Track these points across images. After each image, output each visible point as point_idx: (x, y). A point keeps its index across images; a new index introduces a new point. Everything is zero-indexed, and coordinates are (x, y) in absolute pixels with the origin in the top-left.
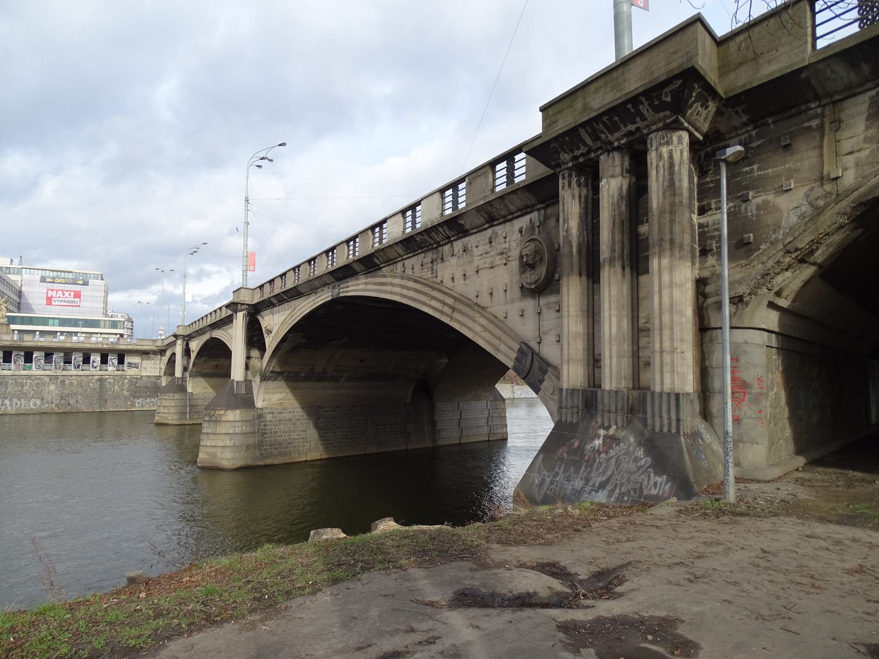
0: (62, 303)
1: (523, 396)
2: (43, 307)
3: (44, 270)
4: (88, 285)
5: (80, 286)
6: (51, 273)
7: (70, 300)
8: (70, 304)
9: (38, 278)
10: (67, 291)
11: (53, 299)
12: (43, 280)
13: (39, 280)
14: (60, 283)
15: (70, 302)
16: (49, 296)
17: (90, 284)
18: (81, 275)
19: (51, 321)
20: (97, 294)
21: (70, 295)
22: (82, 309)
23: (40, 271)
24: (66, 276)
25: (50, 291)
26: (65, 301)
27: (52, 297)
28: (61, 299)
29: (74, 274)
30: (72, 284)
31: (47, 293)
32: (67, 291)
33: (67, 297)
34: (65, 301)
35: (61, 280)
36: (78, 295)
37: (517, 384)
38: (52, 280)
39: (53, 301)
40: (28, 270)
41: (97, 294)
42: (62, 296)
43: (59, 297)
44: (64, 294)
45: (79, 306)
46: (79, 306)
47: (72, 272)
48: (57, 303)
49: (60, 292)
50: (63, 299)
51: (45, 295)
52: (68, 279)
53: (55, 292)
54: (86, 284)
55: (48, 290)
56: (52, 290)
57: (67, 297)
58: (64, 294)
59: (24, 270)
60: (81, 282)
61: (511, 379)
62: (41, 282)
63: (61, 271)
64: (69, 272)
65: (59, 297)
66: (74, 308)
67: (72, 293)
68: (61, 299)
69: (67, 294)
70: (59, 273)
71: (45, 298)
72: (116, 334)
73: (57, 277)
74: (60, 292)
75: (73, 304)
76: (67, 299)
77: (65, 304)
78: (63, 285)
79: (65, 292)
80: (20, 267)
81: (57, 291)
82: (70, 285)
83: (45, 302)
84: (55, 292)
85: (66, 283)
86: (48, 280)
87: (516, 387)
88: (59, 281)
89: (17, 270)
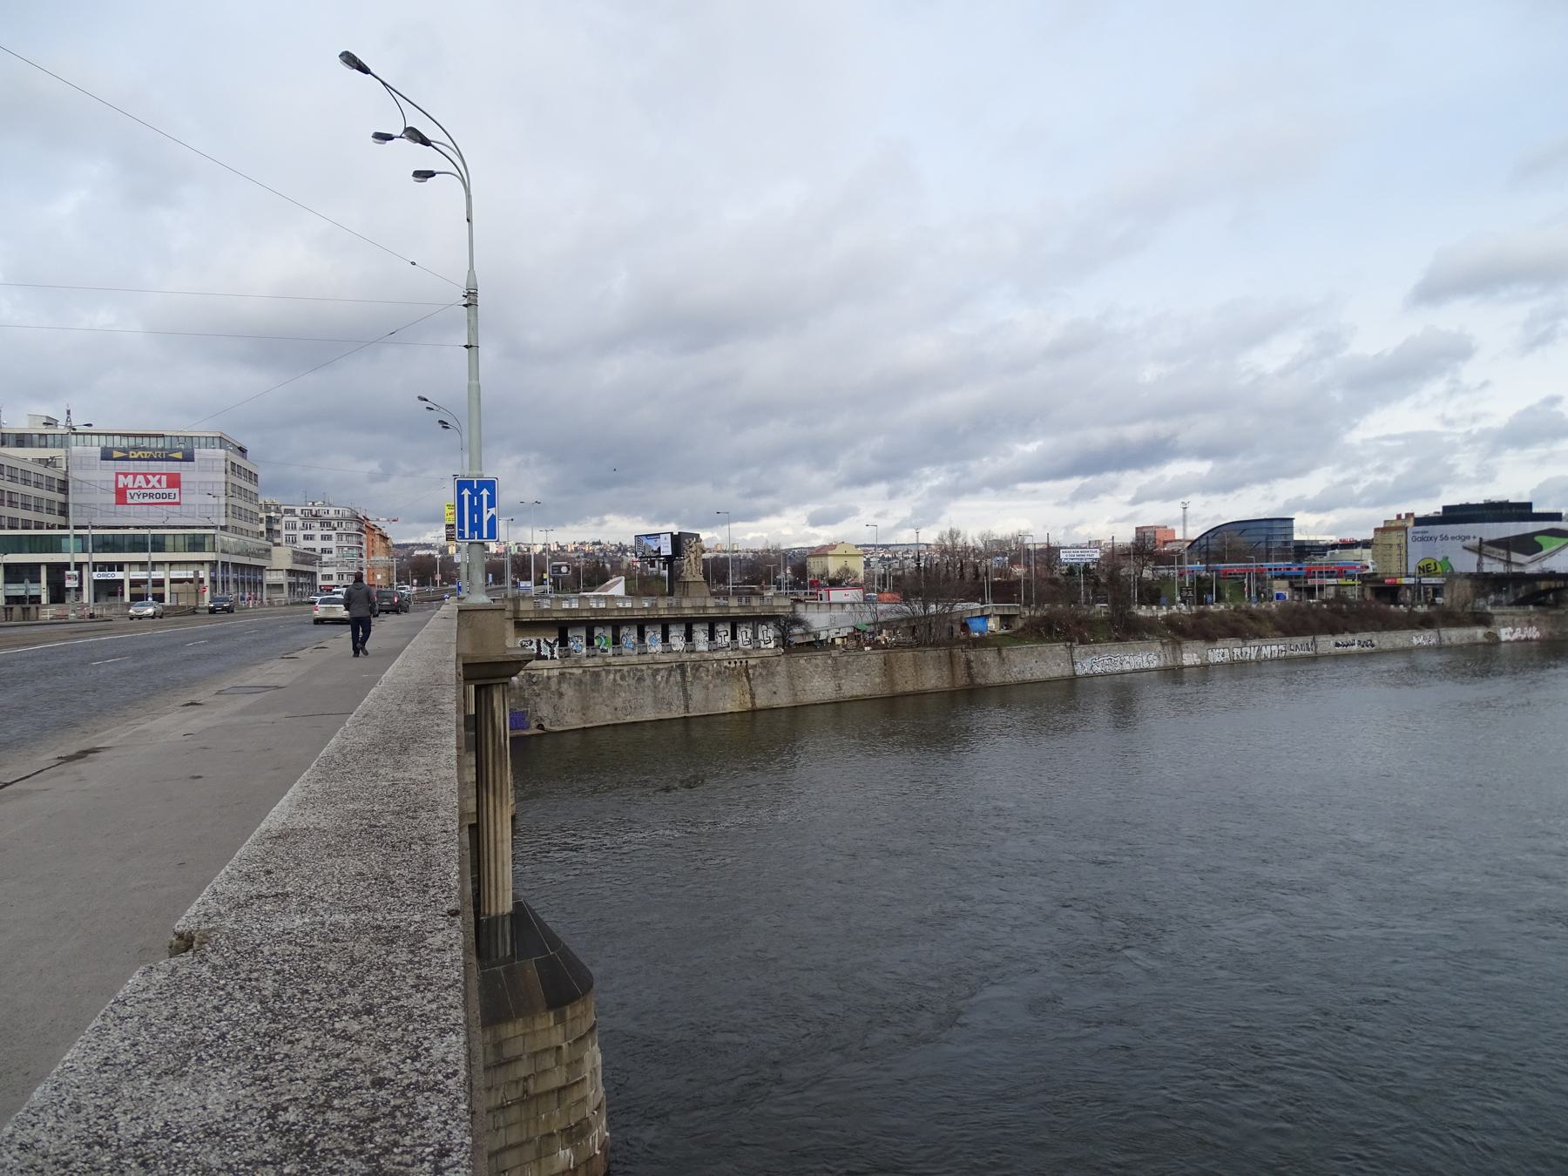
0: (147, 500)
1: (1098, 669)
2: (112, 509)
4: (193, 461)
7: (161, 491)
8: (161, 500)
9: (96, 451)
11: (128, 491)
12: (107, 455)
13: (99, 455)
14: (139, 459)
16: (121, 486)
17: (196, 457)
18: (182, 440)
20: (212, 477)
21: (159, 481)
22: (184, 509)
25: (121, 477)
26: (151, 495)
27: (126, 487)
28: (143, 491)
29: (167, 439)
30: (162, 460)
31: (117, 481)
34: (151, 495)
35: (140, 453)
36: (174, 481)
37: (1083, 642)
38: (122, 455)
39: (128, 496)
41: (212, 477)
42: (144, 485)
43: (140, 488)
44: (148, 482)
45: (179, 504)
46: (179, 504)
47: (163, 436)
50: (148, 491)
51: (113, 485)
52: (153, 450)
53: (130, 477)
54: (188, 457)
55: (117, 474)
56: (126, 475)
57: (154, 487)
58: (148, 482)
60: (179, 455)
61: (1068, 629)
62: (103, 459)
63: (142, 436)
64: (157, 436)
65: (140, 488)
66: (170, 508)
67: (164, 478)
68: (143, 491)
69: (154, 481)
70: (139, 440)
71: (114, 491)
72: (202, 563)
73: (135, 449)
75: (167, 500)
76: (154, 491)
77: (151, 501)
79: (150, 477)
81: (135, 475)
83: (112, 498)
84: (130, 477)
85: (151, 459)
86: (116, 454)
87: (1079, 650)
88: (136, 456)
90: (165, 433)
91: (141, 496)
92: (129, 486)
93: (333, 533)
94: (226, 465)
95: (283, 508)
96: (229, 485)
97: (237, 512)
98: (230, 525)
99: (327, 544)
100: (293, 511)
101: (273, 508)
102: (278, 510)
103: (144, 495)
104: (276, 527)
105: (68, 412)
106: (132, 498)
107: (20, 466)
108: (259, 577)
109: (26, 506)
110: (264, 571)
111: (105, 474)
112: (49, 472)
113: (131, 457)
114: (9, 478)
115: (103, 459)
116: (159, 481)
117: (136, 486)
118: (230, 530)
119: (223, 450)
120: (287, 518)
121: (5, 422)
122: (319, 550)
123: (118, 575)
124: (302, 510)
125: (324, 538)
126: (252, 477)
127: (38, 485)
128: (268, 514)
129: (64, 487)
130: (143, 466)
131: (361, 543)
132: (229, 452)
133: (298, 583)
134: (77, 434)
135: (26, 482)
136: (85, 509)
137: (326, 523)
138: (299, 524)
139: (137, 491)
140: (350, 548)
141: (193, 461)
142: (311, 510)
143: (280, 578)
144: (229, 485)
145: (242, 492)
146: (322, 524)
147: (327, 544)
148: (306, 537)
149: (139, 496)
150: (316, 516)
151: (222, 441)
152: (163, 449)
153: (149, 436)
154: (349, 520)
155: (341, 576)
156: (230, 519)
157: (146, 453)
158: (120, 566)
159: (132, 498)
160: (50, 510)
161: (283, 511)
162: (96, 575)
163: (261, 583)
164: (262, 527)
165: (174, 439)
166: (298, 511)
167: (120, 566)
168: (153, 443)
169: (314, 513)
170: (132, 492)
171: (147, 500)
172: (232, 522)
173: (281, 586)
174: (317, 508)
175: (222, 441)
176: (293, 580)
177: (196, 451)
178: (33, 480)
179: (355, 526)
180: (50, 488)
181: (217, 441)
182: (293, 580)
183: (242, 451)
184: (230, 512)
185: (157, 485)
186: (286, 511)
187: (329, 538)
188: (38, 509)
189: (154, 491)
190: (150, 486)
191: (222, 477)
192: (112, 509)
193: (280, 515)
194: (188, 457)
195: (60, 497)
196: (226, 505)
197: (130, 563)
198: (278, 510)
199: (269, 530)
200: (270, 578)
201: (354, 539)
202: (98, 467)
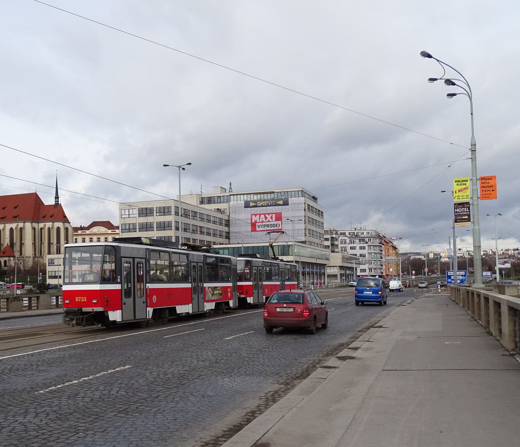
2: (249, 234)
3: (249, 194)
4: (288, 205)
5: (280, 207)
7: (272, 223)
10: (269, 214)
11: (257, 224)
12: (247, 205)
13: (243, 205)
14: (262, 206)
15: (273, 225)
16: (253, 221)
18: (283, 194)
21: (272, 218)
23: (242, 196)
24: (266, 198)
26: (268, 226)
27: (256, 222)
28: (264, 224)
29: (276, 194)
30: (273, 206)
32: (269, 214)
33: (262, 222)
34: (268, 226)
35: (262, 203)
36: (279, 217)
38: (254, 204)
39: (257, 227)
40: (235, 196)
42: (264, 220)
44: (266, 218)
47: (273, 192)
48: (261, 229)
49: (262, 216)
50: (266, 223)
52: (267, 200)
53: (258, 216)
54: (286, 203)
55: (252, 215)
56: (256, 215)
57: (269, 221)
58: (266, 218)
59: (232, 197)
60: (281, 202)
62: (245, 207)
63: (264, 193)
64: (271, 193)
65: (262, 222)
67: (274, 216)
68: (264, 224)
69: (269, 217)
73: (261, 201)
74: (262, 216)
76: (269, 223)
78: (264, 208)
79: (267, 215)
81: (260, 215)
82: (271, 207)
83: (250, 228)
84: (258, 216)
85: (268, 205)
86: (252, 204)
88: (260, 205)
89: (226, 198)
90: (275, 191)
91: (263, 227)
92: (258, 221)
93: (366, 245)
94: (305, 206)
95: (339, 232)
96: (307, 217)
97: (311, 233)
98: (307, 240)
99: (363, 252)
100: (344, 234)
101: (334, 232)
102: (337, 234)
103: (265, 226)
104: (336, 243)
105: (230, 184)
106: (259, 228)
107: (209, 213)
108: (323, 271)
109: (208, 234)
110: (326, 267)
111: (246, 215)
112: (219, 215)
113: (258, 205)
114: (200, 219)
115: (245, 207)
116: (272, 218)
117: (260, 221)
118: (307, 243)
119: (303, 198)
121: (203, 192)
122: (358, 255)
124: (349, 233)
125: (361, 248)
126: (320, 213)
127: (214, 222)
128: (332, 236)
129: (228, 224)
130: (264, 210)
131: (381, 251)
132: (306, 199)
133: (346, 274)
134: (234, 195)
135: (209, 221)
136: (237, 235)
137: (362, 240)
138: (348, 241)
139: (261, 224)
140: (375, 253)
141: (288, 205)
142: (354, 233)
143: (335, 271)
144: (307, 217)
145: (312, 221)
146: (360, 241)
147: (363, 252)
148: (351, 248)
149: (262, 226)
150: (357, 236)
152: (273, 200)
153: (267, 193)
154: (374, 238)
155: (370, 270)
156: (307, 237)
157: (265, 202)
159: (259, 228)
160: (221, 236)
161: (339, 234)
163: (324, 274)
164: (328, 243)
165: (279, 194)
166: (347, 234)
168: (269, 196)
169: (355, 234)
170: (259, 224)
172: (308, 239)
173: (335, 276)
174: (357, 231)
175: (303, 193)
176: (343, 272)
177: (290, 199)
178: (212, 220)
179: (378, 241)
180: (221, 224)
181: (300, 193)
182: (343, 272)
183: (315, 199)
184: (307, 233)
185: (271, 220)
186: (341, 234)
187: (364, 248)
188: (215, 235)
189: (269, 223)
190: (267, 220)
191: (302, 213)
192: (249, 234)
193: (338, 236)
194: (286, 203)
195: (226, 229)
196: (305, 229)
198: (337, 234)
199: (332, 245)
200: (329, 271)
201: (378, 248)
202: (243, 212)
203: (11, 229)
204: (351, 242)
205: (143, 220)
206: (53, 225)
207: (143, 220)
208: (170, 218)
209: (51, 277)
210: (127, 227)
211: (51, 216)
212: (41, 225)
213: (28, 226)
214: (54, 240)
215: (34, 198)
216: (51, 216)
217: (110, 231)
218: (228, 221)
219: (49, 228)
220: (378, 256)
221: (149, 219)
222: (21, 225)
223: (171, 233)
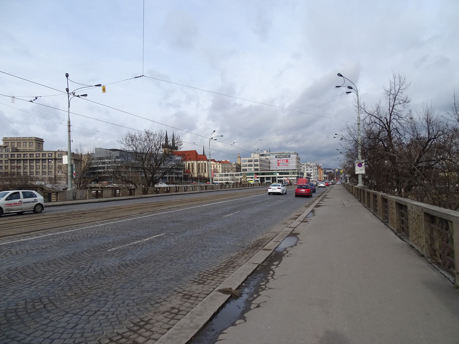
0: (283, 165)
6: (279, 154)
12: (276, 157)
15: (285, 164)
19: (274, 173)
26: (283, 164)
27: (279, 163)
34: (283, 164)
36: (287, 161)
44: (283, 161)
48: (281, 165)
54: (289, 157)
58: (283, 161)
69: (284, 161)
70: (281, 154)
74: (282, 161)
80: (269, 153)
81: (281, 160)
83: (277, 165)
85: (283, 157)
86: (278, 157)
93: (312, 169)
99: (311, 171)
120: (303, 166)
122: (309, 173)
123: (282, 179)
125: (310, 170)
137: (311, 167)
138: (305, 167)
140: (316, 172)
147: (311, 171)
148: (307, 170)
151: (295, 153)
154: (315, 166)
155: (314, 178)
158: (282, 177)
162: (278, 179)
166: (305, 165)
167: (282, 177)
171: (283, 165)
179: (317, 167)
186: (303, 165)
187: (312, 170)
194: (289, 157)
197: (284, 177)
201: (317, 170)
203: (189, 164)
204: (307, 168)
205: (249, 163)
206: (203, 162)
207: (249, 163)
208: (258, 163)
209: (215, 180)
210: (244, 165)
211: (202, 159)
212: (199, 162)
213: (195, 162)
214: (203, 167)
215: (195, 152)
216: (202, 159)
217: (215, 163)
218: (270, 162)
219: (202, 163)
220: (317, 173)
221: (251, 163)
222: (193, 162)
223: (258, 167)
